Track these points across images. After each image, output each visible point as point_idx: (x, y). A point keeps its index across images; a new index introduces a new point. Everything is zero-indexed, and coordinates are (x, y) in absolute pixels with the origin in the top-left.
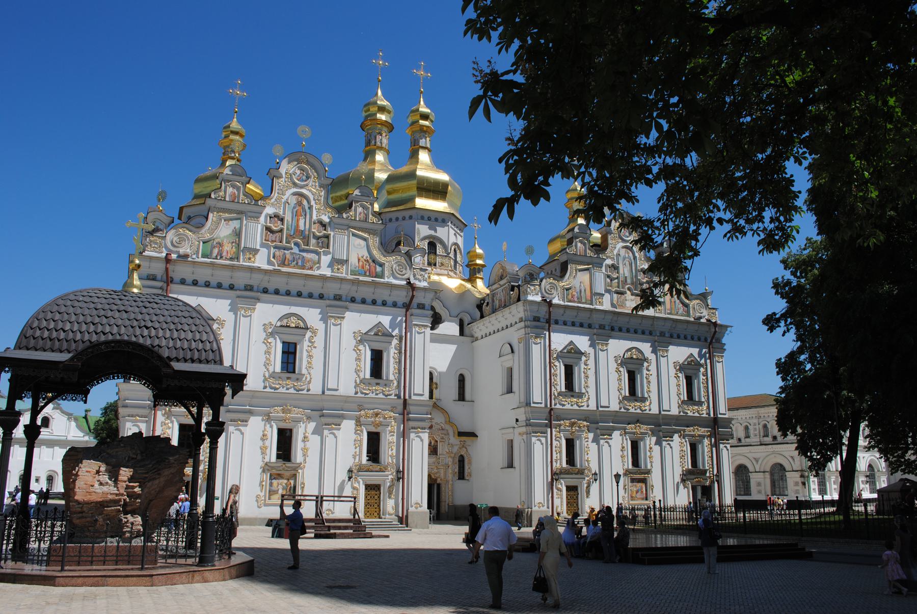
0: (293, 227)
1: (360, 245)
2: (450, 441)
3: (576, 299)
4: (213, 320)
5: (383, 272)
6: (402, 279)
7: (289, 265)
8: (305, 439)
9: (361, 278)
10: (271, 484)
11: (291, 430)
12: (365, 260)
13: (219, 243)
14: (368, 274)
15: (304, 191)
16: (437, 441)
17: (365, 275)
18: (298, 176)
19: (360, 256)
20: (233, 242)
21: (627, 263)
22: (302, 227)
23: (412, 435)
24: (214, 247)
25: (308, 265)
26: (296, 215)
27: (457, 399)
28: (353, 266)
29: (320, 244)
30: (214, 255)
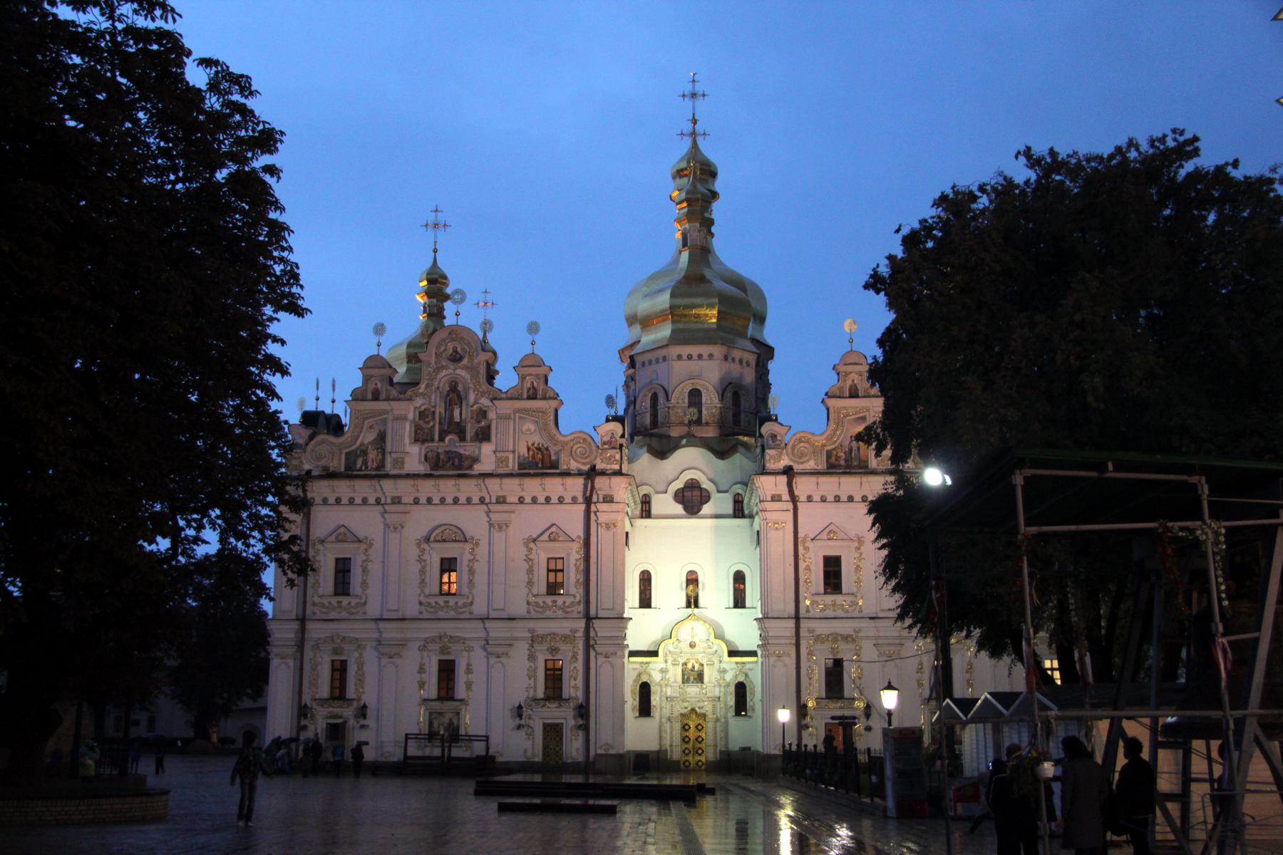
0: (447, 420)
1: (529, 430)
2: (723, 666)
3: (843, 463)
4: (360, 541)
5: (558, 460)
8: (469, 670)
9: (532, 471)
10: (431, 724)
11: (453, 662)
12: (537, 449)
14: (540, 465)
15: (459, 371)
16: (702, 665)
17: (537, 467)
18: (451, 355)
19: (530, 444)
20: (378, 449)
22: (457, 419)
23: (601, 659)
24: (358, 456)
27: (732, 604)
28: (521, 458)
29: (480, 436)
30: (358, 466)
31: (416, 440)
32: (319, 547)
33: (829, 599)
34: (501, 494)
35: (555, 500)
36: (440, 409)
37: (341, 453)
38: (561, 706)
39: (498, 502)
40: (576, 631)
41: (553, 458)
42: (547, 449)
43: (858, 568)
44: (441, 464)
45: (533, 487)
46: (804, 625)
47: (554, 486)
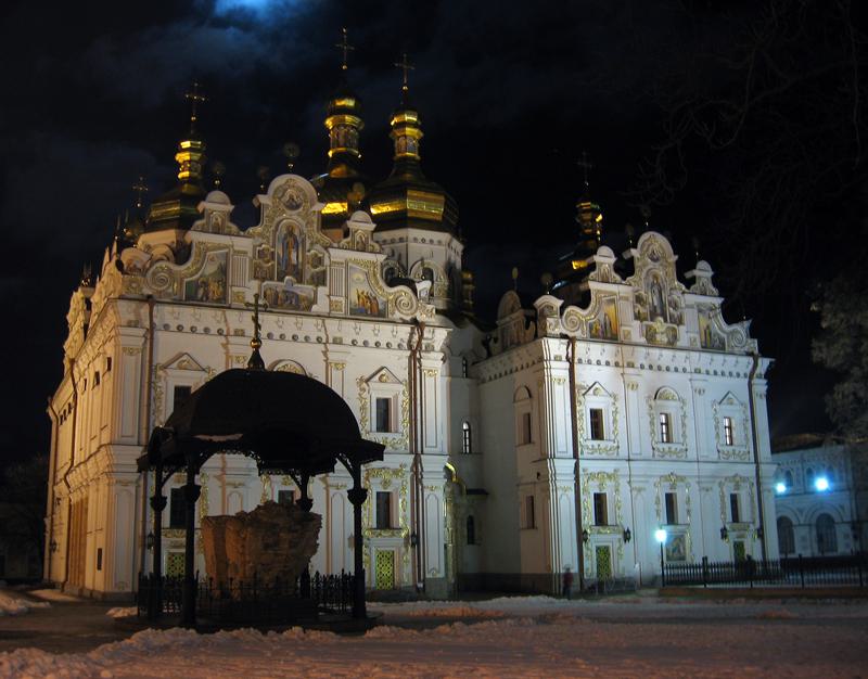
1: (358, 279)
6: (407, 315)
7: (282, 305)
13: (203, 282)
17: (367, 315)
21: (656, 291)
25: (303, 304)
26: (286, 247)
30: (200, 296)
31: (256, 278)
32: (160, 373)
33: (596, 443)
34: (338, 335)
35: (384, 345)
36: (279, 250)
37: (181, 284)
38: (393, 535)
39: (335, 342)
40: (405, 466)
41: (380, 307)
42: (375, 298)
43: (615, 421)
44: (279, 302)
45: (367, 330)
46: (582, 464)
47: (385, 332)
